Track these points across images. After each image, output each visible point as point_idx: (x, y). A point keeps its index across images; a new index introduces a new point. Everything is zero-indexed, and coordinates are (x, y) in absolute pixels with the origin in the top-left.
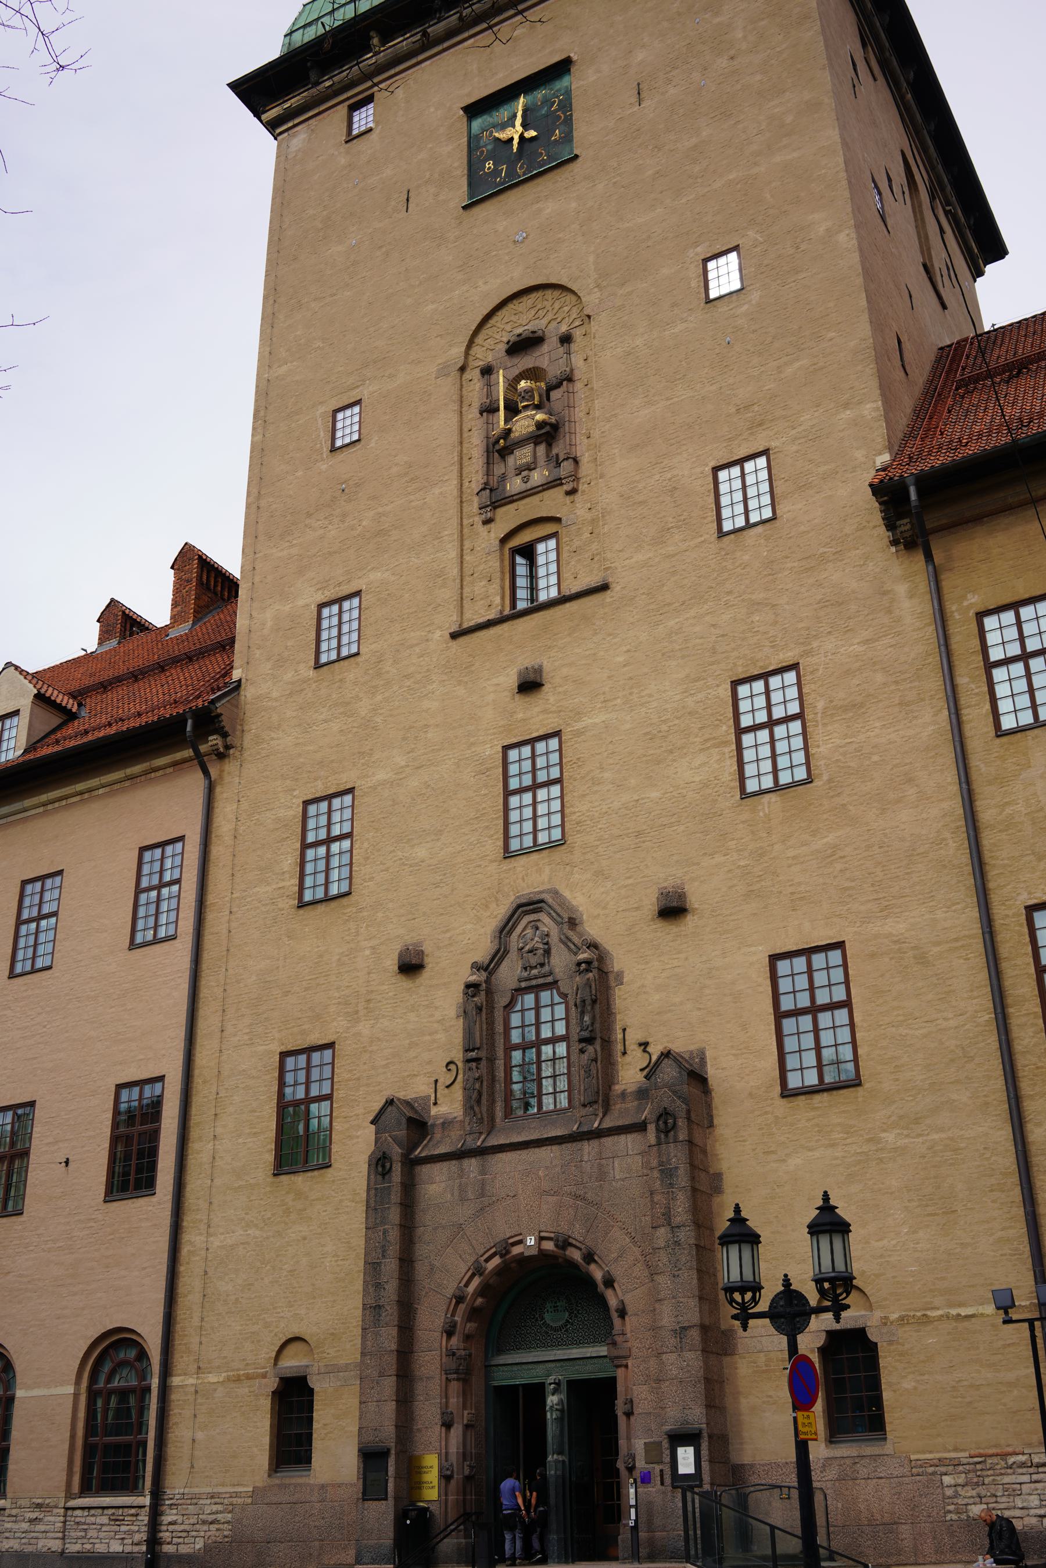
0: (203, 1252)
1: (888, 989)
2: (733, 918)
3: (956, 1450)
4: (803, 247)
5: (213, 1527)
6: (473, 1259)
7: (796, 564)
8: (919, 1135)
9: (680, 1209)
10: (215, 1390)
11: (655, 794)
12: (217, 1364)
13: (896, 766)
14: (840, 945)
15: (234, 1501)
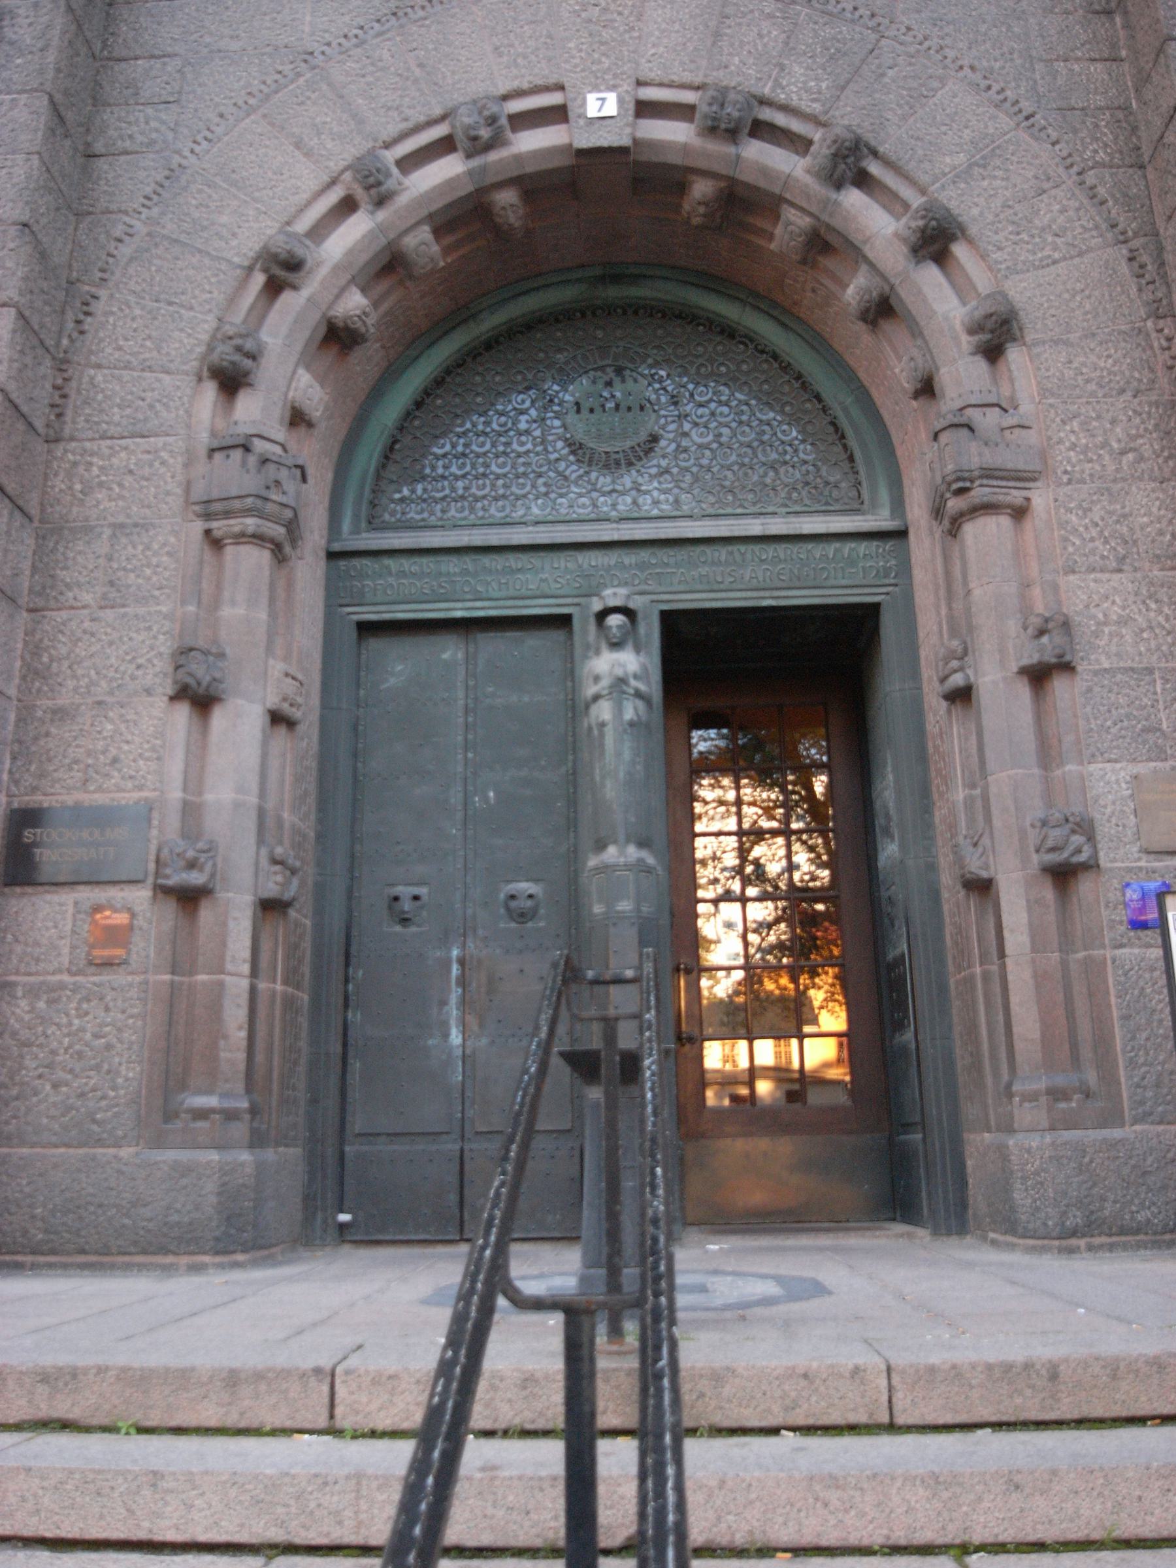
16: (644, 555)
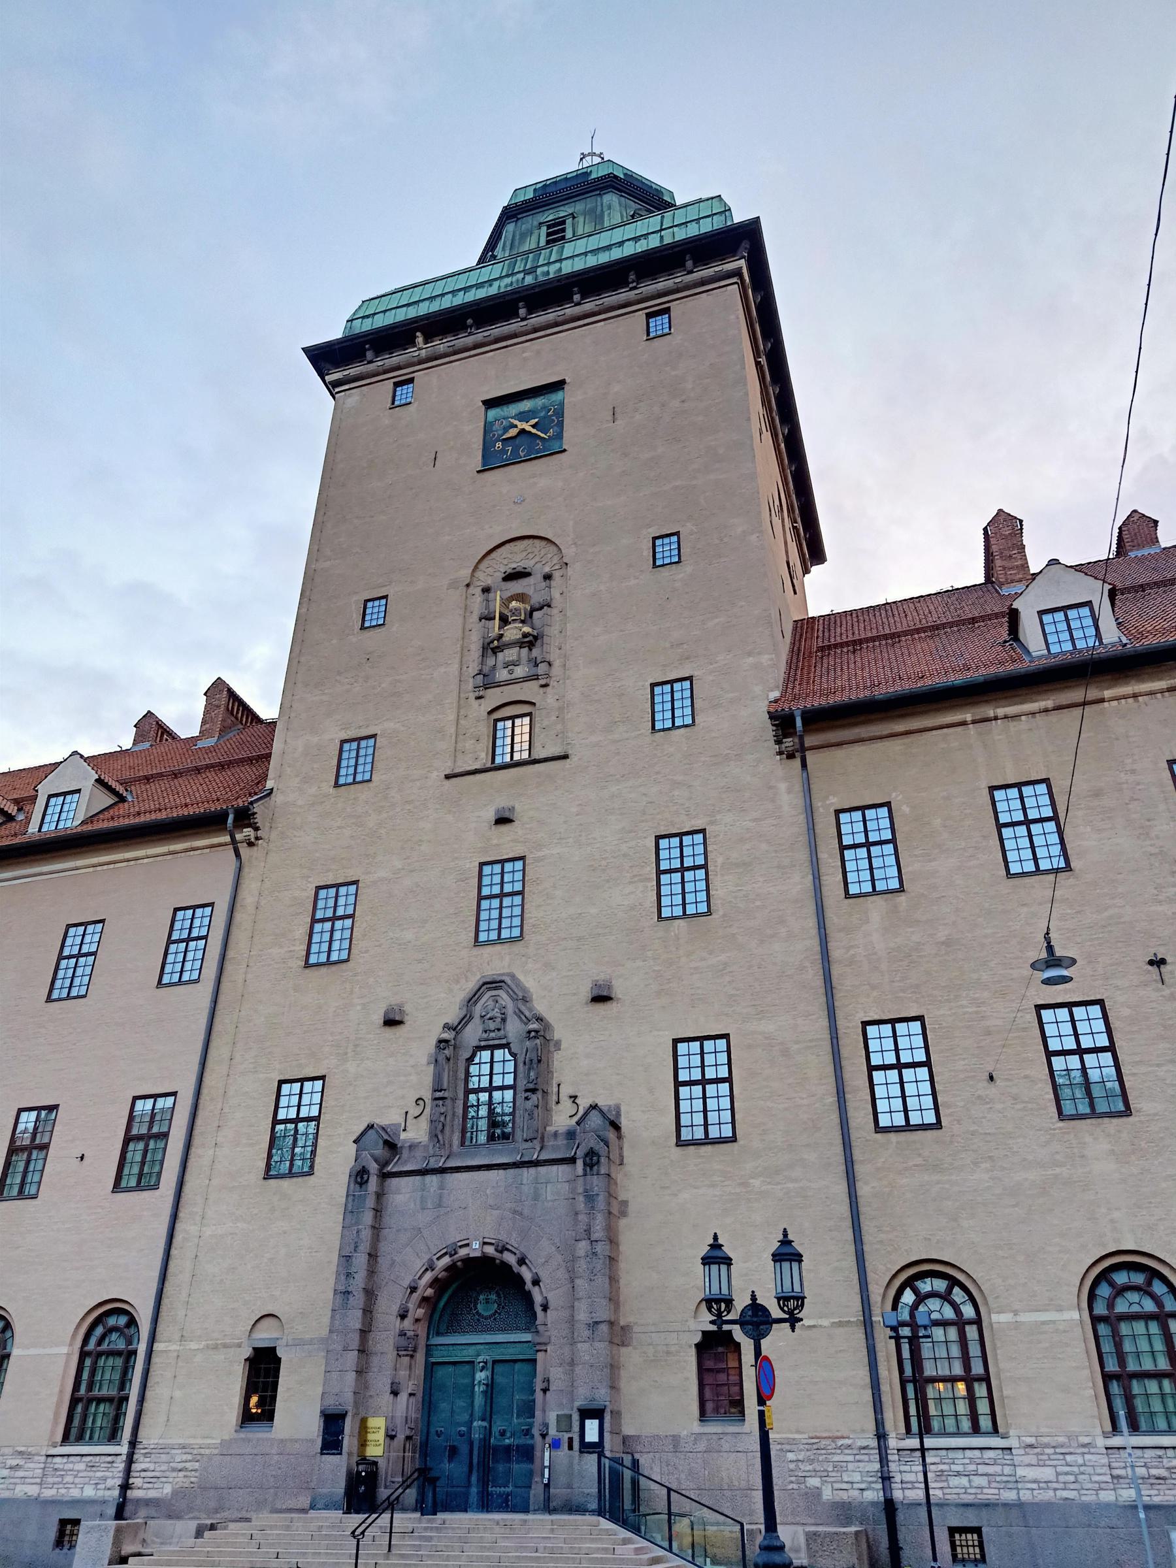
0: (196, 1240)
1: (760, 1071)
2: (647, 1008)
3: (798, 1432)
4: (725, 540)
5: (181, 1474)
6: (428, 1257)
7: (707, 759)
8: (778, 1184)
9: (598, 1228)
10: (195, 1355)
11: (593, 911)
12: (198, 1334)
13: (773, 911)
14: (726, 1036)
15: (202, 1451)
16: (491, 1346)
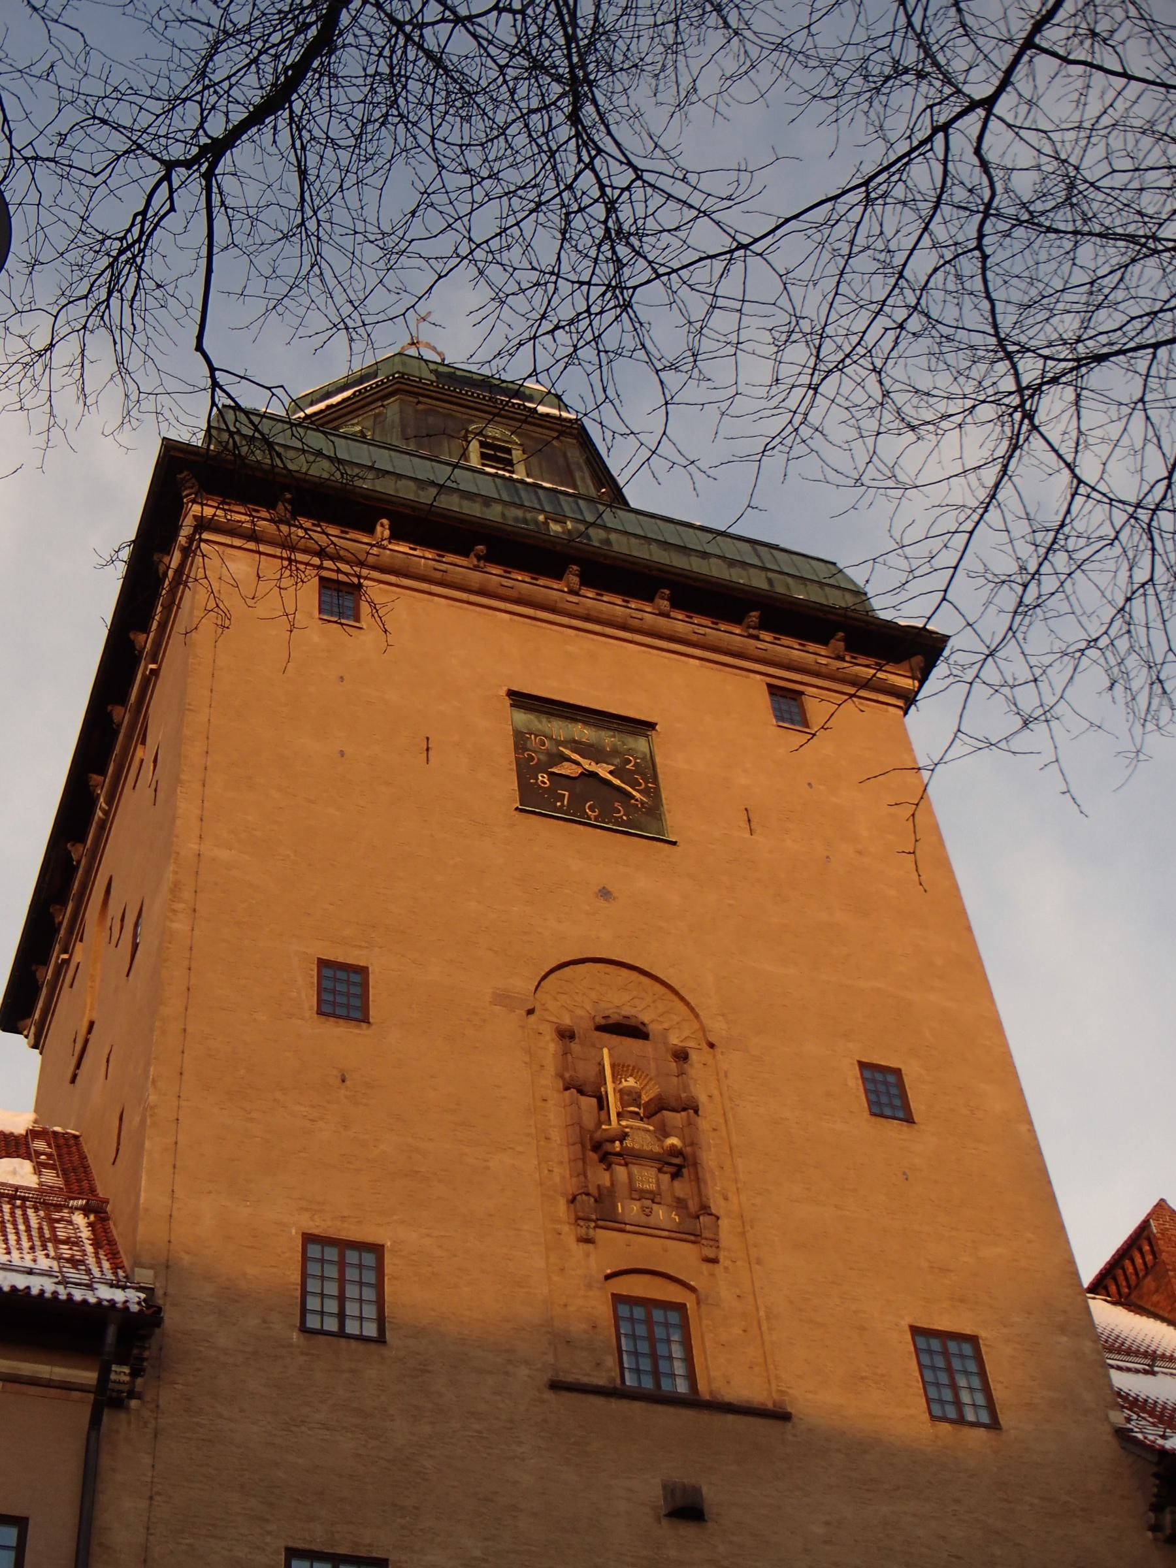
7: (1036, 1501)
